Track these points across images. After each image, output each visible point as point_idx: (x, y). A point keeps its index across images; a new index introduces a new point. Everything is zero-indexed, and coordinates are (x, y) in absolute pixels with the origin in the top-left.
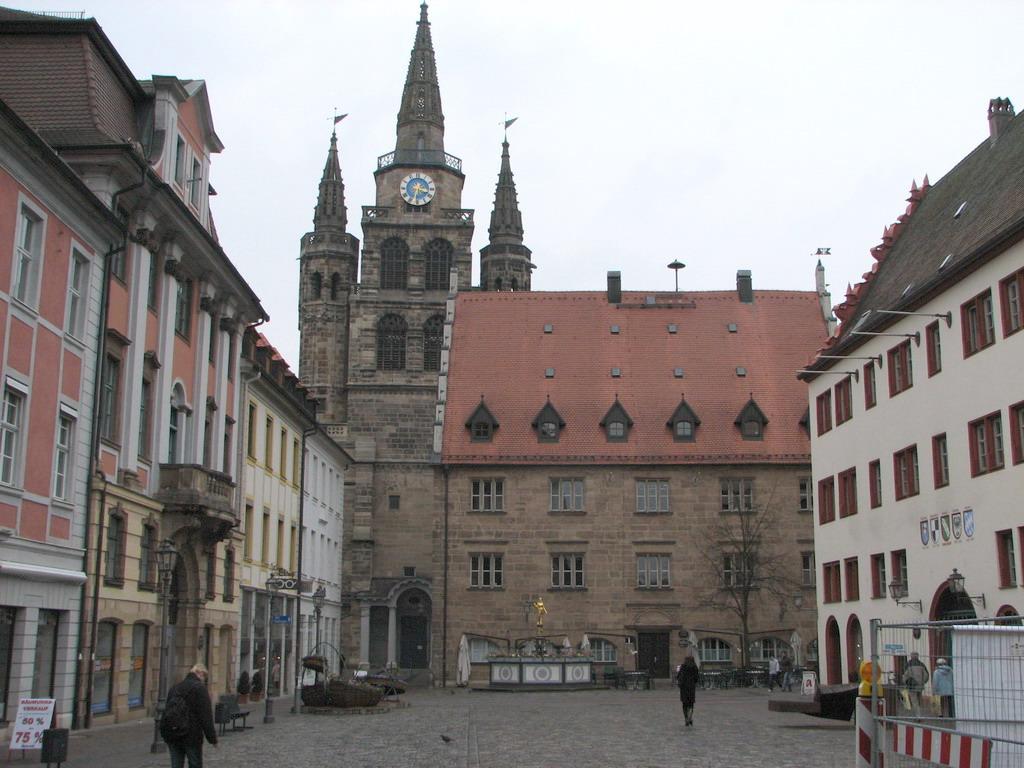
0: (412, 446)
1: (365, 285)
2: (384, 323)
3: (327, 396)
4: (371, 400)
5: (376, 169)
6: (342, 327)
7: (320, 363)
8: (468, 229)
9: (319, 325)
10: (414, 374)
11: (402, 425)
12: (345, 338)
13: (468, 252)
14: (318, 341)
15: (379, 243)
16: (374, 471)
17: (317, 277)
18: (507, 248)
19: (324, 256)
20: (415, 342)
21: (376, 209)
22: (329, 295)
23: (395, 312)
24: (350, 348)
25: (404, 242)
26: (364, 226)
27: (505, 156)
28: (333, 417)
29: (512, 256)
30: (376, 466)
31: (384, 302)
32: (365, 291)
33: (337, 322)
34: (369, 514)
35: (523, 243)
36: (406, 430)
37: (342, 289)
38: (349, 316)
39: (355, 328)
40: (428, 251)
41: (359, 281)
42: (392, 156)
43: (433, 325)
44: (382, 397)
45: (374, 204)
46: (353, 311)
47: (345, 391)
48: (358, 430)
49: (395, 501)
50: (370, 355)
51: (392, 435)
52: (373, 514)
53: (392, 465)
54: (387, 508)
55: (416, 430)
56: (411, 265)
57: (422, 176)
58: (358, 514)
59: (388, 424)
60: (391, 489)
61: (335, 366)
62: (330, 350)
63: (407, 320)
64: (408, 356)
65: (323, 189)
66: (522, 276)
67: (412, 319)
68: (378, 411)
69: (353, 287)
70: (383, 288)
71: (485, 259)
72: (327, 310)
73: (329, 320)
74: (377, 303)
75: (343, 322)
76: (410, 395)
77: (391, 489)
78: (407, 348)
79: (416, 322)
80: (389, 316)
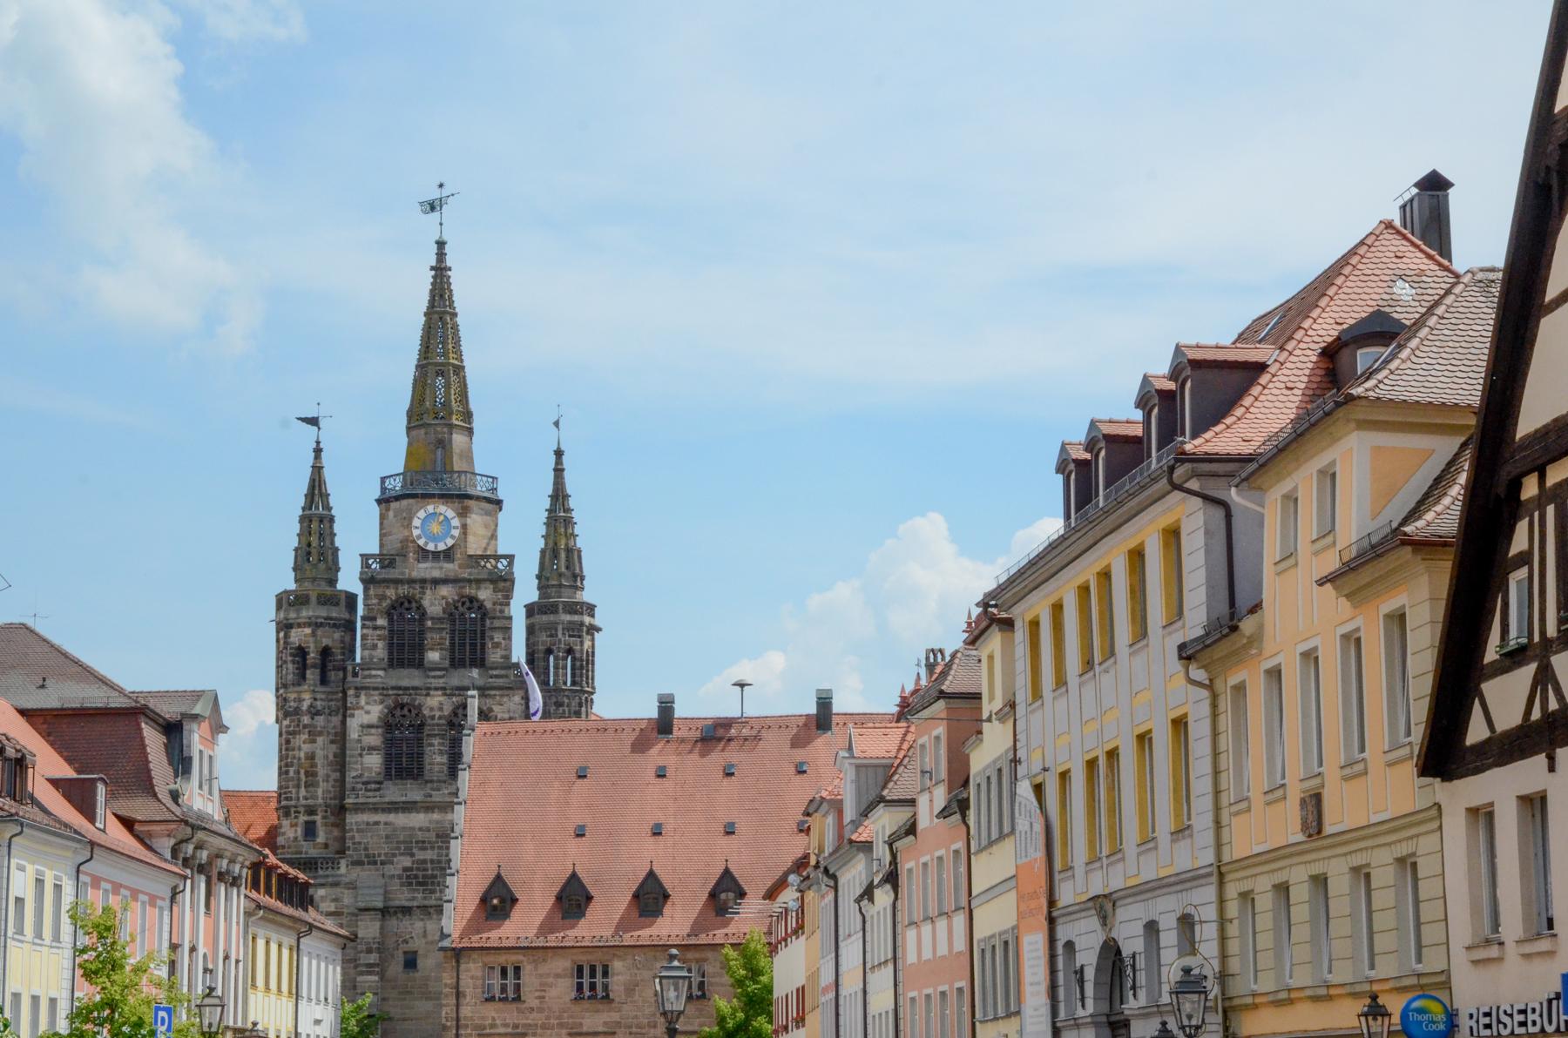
0: (433, 883)
1: (366, 665)
2: (393, 715)
3: (318, 818)
4: (377, 823)
5: (377, 494)
6: (336, 720)
7: (307, 774)
8: (504, 583)
9: (306, 720)
11: (420, 855)
12: (341, 737)
13: (506, 614)
14: (304, 743)
15: (384, 605)
16: (383, 916)
17: (301, 652)
18: (561, 607)
19: (309, 625)
20: (436, 741)
22: (318, 677)
23: (406, 699)
24: (348, 752)
25: (419, 603)
26: (363, 580)
27: (559, 471)
28: (326, 846)
29: (567, 618)
30: (385, 912)
31: (393, 688)
32: (367, 673)
33: (330, 714)
34: (376, 978)
35: (586, 596)
36: (424, 861)
37: (336, 669)
38: (346, 708)
39: (354, 724)
40: (451, 614)
41: (358, 660)
42: (399, 480)
44: (391, 817)
45: (378, 552)
46: (351, 700)
47: (341, 810)
48: (359, 863)
49: (411, 963)
50: (374, 762)
51: (405, 869)
52: (382, 979)
53: (406, 911)
54: (400, 968)
55: (439, 862)
56: (429, 635)
57: (442, 508)
58: (360, 979)
60: (406, 942)
61: (328, 776)
62: (320, 753)
63: (426, 712)
64: (427, 760)
66: (582, 643)
67: (432, 709)
68: (387, 837)
69: (350, 668)
71: (532, 620)
72: (315, 699)
73: (318, 713)
74: (383, 689)
76: (430, 815)
77: (406, 942)
78: (428, 749)
79: (437, 714)
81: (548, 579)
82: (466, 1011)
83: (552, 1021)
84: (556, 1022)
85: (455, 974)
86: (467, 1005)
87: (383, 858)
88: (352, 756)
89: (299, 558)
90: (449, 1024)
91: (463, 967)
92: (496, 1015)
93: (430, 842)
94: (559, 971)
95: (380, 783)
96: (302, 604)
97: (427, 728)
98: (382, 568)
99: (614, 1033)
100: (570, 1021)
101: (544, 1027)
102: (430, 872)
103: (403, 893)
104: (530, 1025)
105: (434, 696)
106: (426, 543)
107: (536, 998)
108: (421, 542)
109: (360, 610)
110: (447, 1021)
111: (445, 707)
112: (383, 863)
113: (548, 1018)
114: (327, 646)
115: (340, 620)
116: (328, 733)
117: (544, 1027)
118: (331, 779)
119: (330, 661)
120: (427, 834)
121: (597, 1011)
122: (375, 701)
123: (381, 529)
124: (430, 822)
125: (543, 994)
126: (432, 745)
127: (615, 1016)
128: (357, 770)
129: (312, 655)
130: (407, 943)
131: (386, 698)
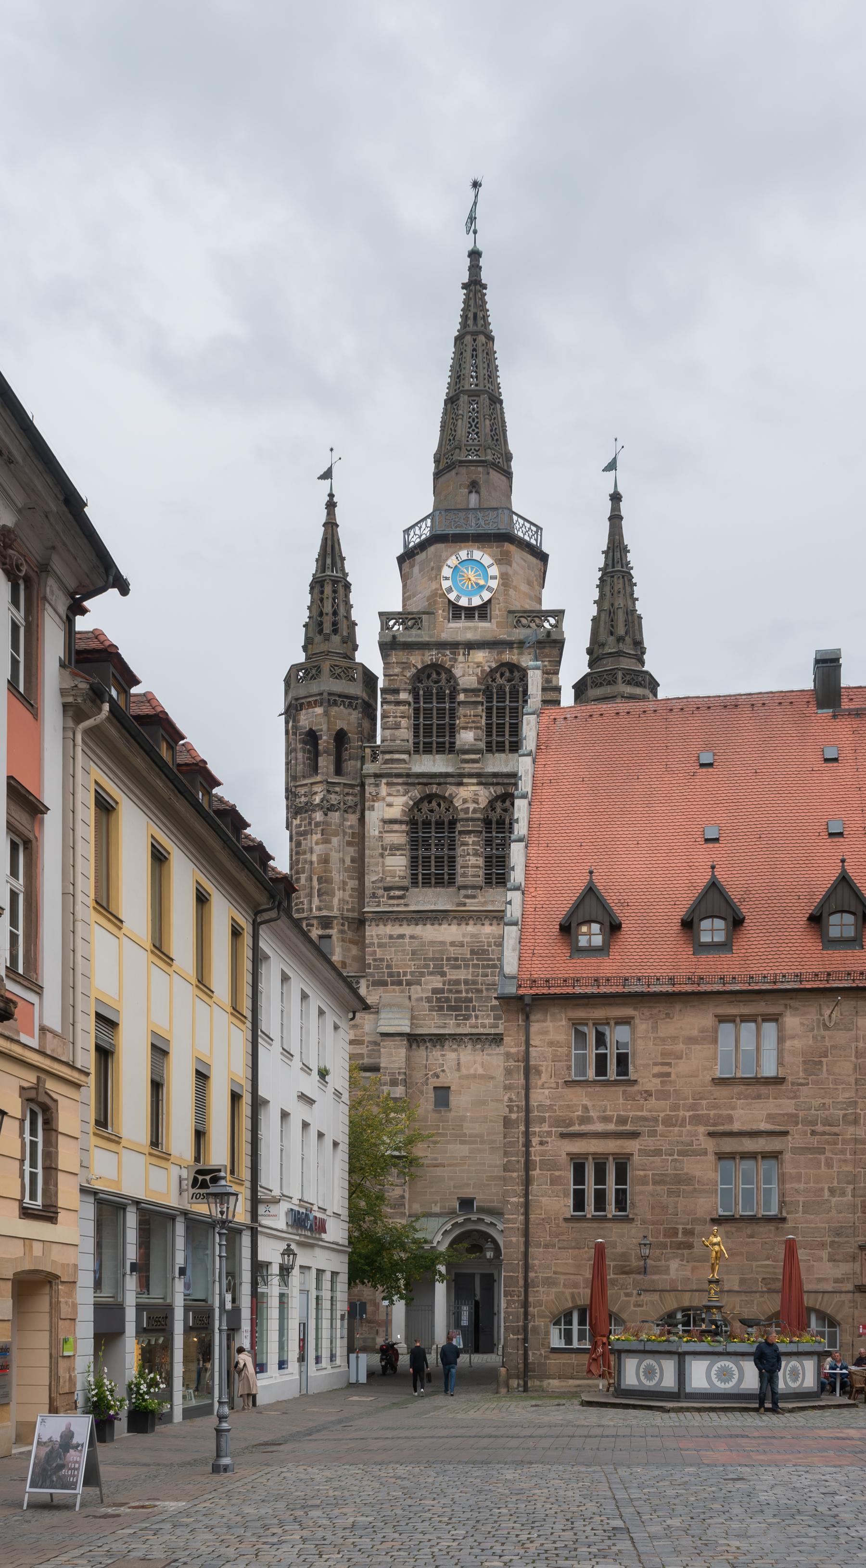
0: (467, 1008)
2: (419, 810)
3: (334, 932)
4: (402, 936)
5: (400, 551)
10: (470, 892)
11: (453, 975)
15: (408, 674)
18: (620, 675)
20: (470, 839)
21: (403, 617)
23: (434, 789)
25: (449, 671)
30: (413, 1040)
32: (388, 756)
36: (457, 982)
43: (499, 810)
46: (369, 789)
49: (442, 1095)
50: (398, 864)
51: (435, 991)
53: (439, 1040)
54: (430, 1106)
55: (475, 983)
56: (462, 711)
59: (431, 974)
63: (458, 803)
64: (460, 861)
65: (316, 591)
67: (465, 801)
68: (414, 953)
70: (417, 752)
75: (354, 812)
76: (463, 926)
78: (460, 851)
79: (472, 806)
80: (429, 798)
81: (603, 645)
82: (540, 1096)
83: (681, 1113)
84: (688, 1114)
85: (523, 1039)
86: (543, 1087)
87: (409, 977)
88: (372, 857)
89: (310, 629)
90: (514, 1116)
91: (535, 1027)
92: (589, 1104)
93: (463, 959)
94: (695, 1033)
95: (406, 889)
96: (313, 678)
97: (458, 825)
98: (406, 629)
99: (785, 1133)
100: (712, 1113)
101: (669, 1122)
102: (464, 995)
103: (433, 1019)
104: (645, 1119)
105: (467, 785)
106: (458, 597)
107: (654, 1076)
108: (452, 596)
109: (380, 684)
110: (511, 1111)
111: (480, 799)
112: (409, 983)
113: (675, 1108)
114: (342, 729)
115: (357, 698)
116: (345, 833)
117: (669, 1122)
118: (348, 887)
119: (346, 749)
120: (460, 950)
121: (759, 1097)
122: (398, 791)
123: (404, 593)
124: (464, 936)
125: (666, 1069)
126: (466, 844)
127: (788, 1106)
128: (377, 873)
129: (324, 738)
130: (438, 1077)
131: (411, 788)
